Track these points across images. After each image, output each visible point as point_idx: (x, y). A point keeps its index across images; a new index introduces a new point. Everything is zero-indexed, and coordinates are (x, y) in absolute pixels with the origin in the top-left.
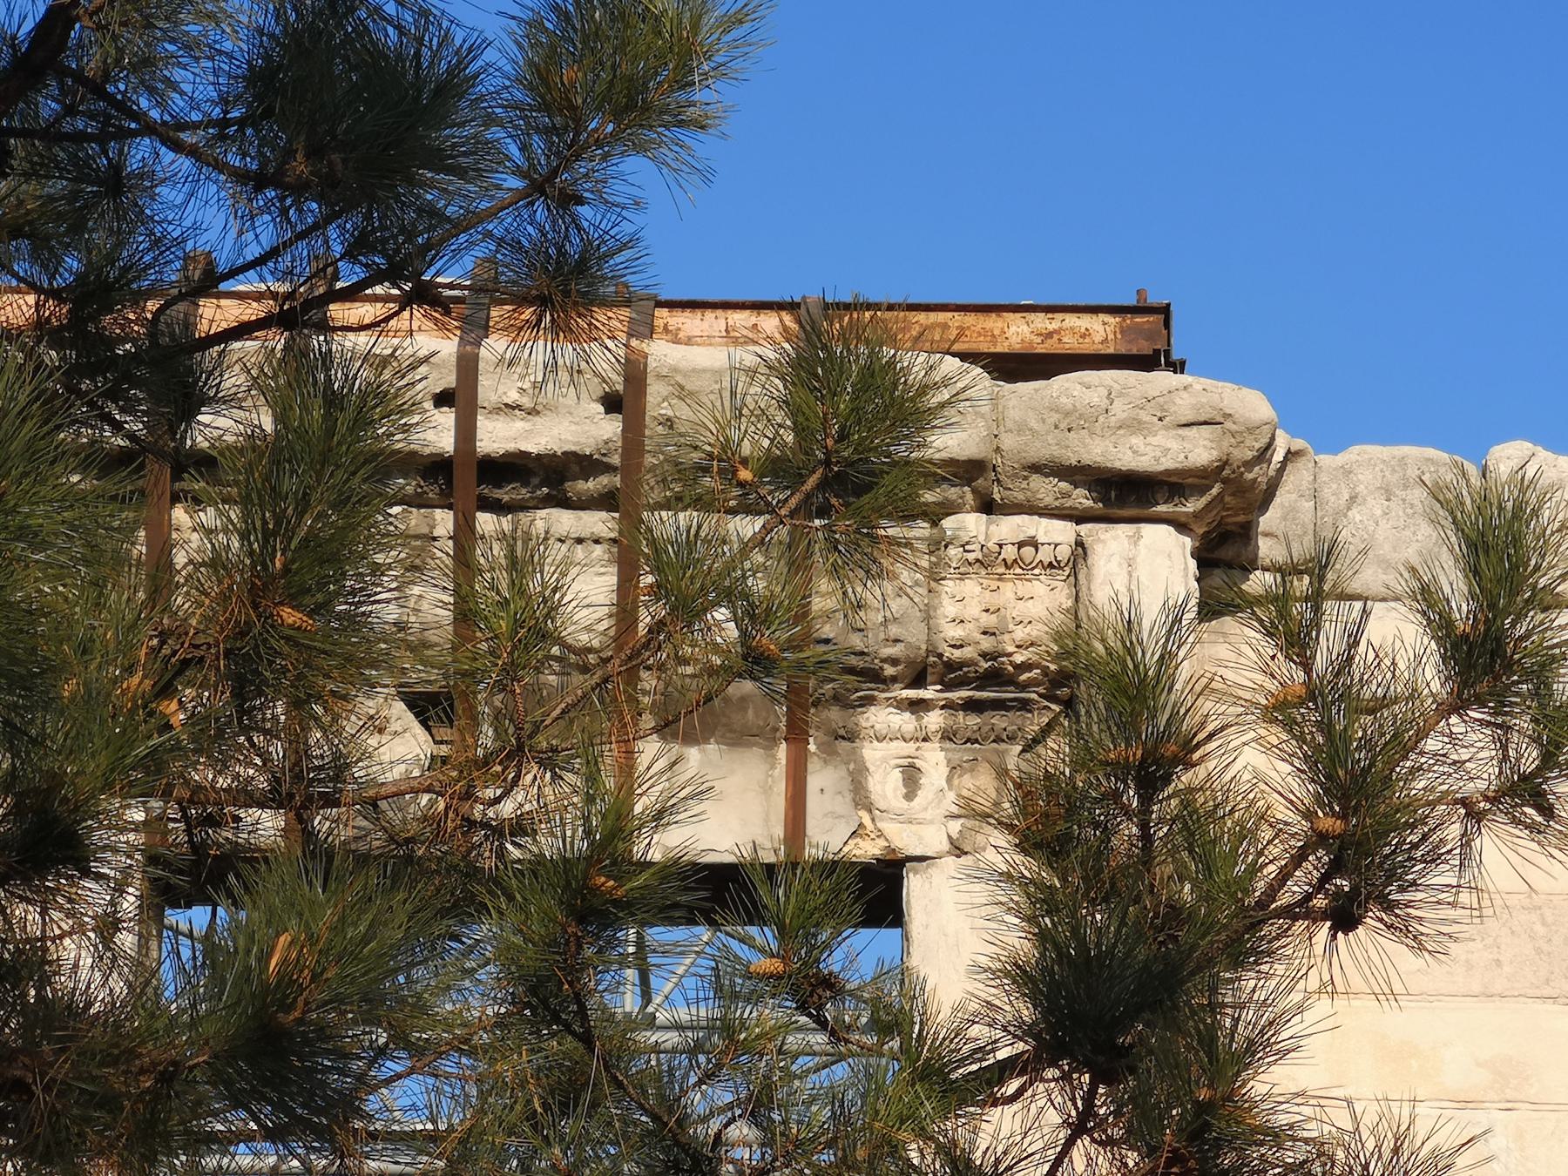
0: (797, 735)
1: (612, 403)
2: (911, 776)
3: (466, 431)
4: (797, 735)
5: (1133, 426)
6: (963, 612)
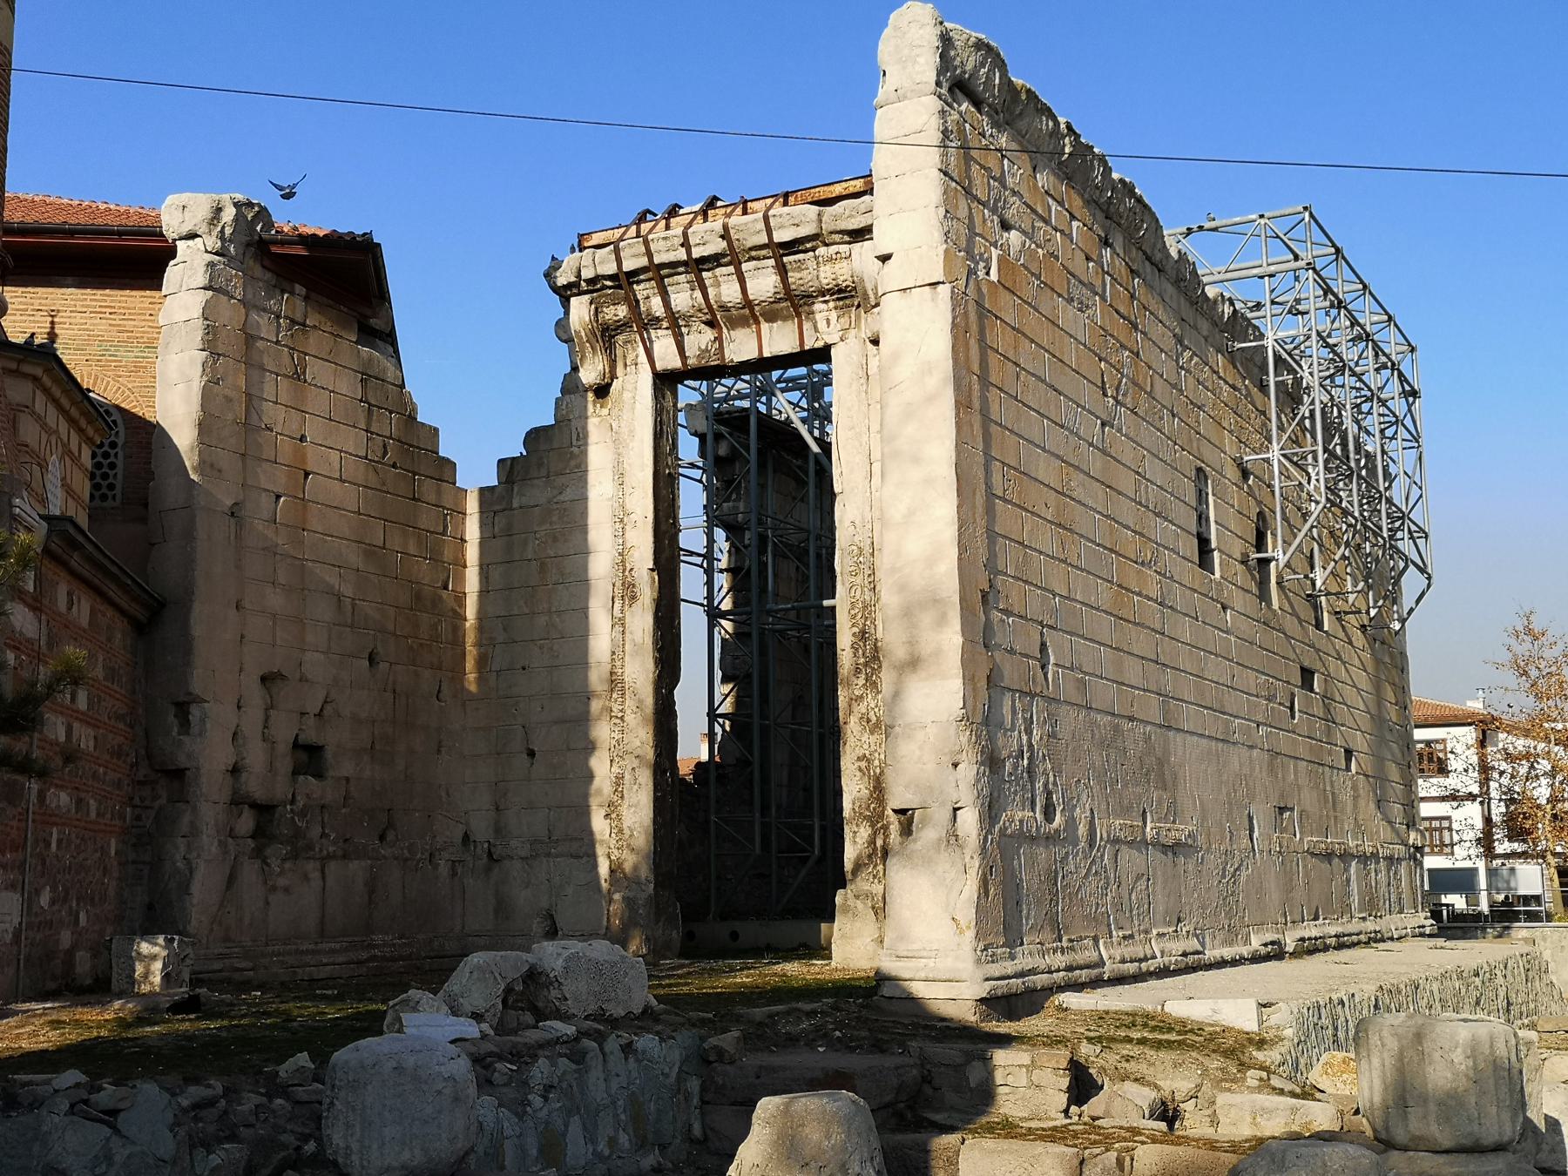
0: (798, 315)
1: (722, 237)
2: (828, 321)
3: (689, 252)
4: (798, 315)
5: (850, 216)
6: (827, 275)
